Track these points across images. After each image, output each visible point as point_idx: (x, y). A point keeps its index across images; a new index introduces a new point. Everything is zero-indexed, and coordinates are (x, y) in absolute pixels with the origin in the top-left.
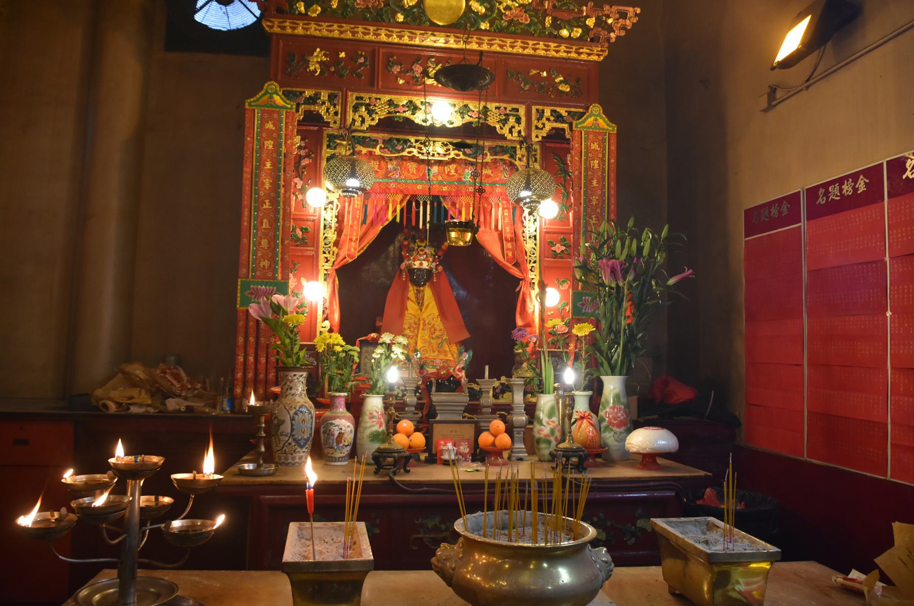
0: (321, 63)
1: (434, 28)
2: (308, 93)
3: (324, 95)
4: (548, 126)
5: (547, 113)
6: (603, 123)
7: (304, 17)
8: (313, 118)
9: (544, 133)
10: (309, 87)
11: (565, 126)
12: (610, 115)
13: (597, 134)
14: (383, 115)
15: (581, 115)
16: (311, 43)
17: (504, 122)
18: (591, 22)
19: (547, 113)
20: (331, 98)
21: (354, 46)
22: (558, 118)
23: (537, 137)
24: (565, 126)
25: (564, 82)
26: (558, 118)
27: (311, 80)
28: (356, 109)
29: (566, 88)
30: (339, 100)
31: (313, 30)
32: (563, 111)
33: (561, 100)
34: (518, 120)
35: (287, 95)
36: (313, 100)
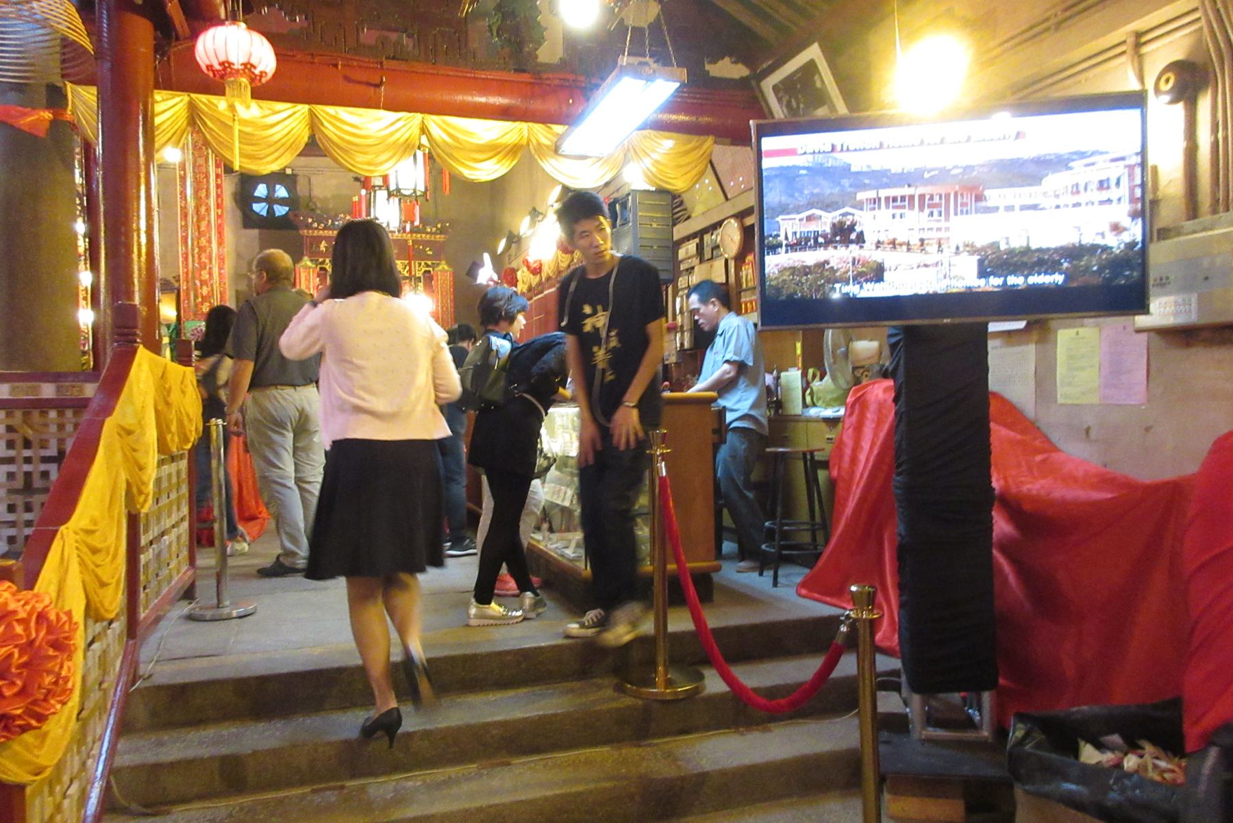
0: (326, 247)
2: (321, 260)
5: (423, 263)
6: (446, 267)
11: (431, 269)
12: (448, 264)
13: (443, 271)
15: (438, 264)
16: (320, 239)
18: (439, 226)
19: (423, 263)
22: (427, 266)
24: (431, 269)
25: (430, 250)
26: (427, 266)
27: (321, 254)
32: (429, 263)
33: (428, 257)
35: (311, 261)
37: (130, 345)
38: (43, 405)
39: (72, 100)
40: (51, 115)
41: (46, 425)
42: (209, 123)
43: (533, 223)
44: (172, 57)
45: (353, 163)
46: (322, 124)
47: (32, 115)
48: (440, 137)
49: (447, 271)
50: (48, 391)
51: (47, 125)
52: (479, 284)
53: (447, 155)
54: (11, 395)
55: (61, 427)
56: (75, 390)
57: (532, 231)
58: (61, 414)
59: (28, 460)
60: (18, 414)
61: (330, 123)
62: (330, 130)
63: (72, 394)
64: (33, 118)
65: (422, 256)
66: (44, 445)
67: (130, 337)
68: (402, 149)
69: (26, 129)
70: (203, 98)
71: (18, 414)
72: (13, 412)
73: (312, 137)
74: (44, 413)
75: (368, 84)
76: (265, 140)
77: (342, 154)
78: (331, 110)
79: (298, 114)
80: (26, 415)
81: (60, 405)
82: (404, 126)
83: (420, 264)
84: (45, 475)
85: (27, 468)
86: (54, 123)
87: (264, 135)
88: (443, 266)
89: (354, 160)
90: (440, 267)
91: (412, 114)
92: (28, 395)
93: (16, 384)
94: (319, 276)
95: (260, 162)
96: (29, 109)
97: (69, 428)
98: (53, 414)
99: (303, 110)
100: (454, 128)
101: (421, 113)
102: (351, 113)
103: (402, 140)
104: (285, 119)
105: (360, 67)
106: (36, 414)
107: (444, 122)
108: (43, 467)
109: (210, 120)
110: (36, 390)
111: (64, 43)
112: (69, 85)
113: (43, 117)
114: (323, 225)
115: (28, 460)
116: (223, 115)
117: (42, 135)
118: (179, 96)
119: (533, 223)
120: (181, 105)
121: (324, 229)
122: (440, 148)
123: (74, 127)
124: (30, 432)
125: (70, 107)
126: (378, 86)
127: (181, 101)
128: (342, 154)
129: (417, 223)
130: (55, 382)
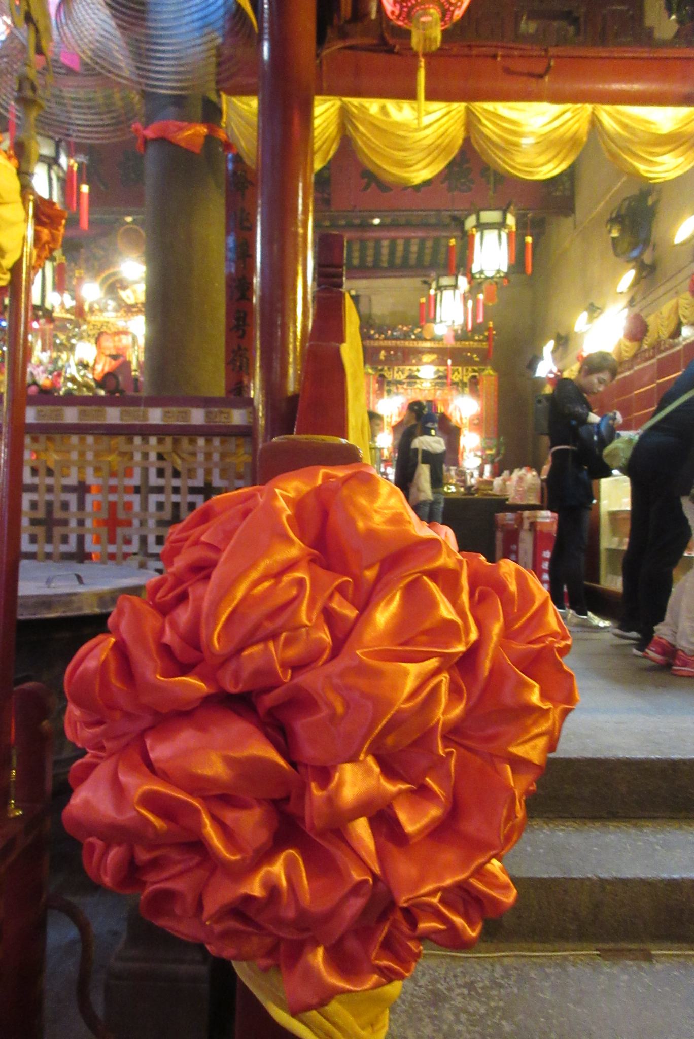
1: (426, 340)
2: (380, 368)
3: (386, 368)
4: (471, 374)
6: (491, 372)
7: (378, 339)
8: (382, 376)
9: (469, 377)
10: (380, 365)
11: (476, 374)
13: (490, 375)
14: (407, 374)
15: (483, 370)
17: (453, 374)
20: (389, 369)
21: (396, 349)
22: (474, 371)
23: (466, 380)
24: (476, 374)
28: (398, 372)
29: (477, 359)
30: (391, 370)
31: (382, 344)
34: (458, 373)
36: (382, 370)
37: (335, 289)
38: (192, 432)
39: (227, 112)
40: (206, 130)
41: (194, 454)
42: (361, 128)
43: (591, 319)
44: (325, 62)
45: (512, 163)
46: (480, 121)
47: (189, 130)
48: (613, 127)
49: (491, 376)
50: (197, 417)
51: (201, 140)
52: (539, 378)
53: (621, 149)
54: (164, 421)
55: (208, 456)
56: (223, 415)
57: (589, 326)
58: (208, 441)
59: (176, 490)
60: (169, 440)
61: (487, 119)
62: (489, 128)
63: (221, 420)
64: (189, 133)
65: (469, 362)
66: (191, 473)
67: (335, 280)
68: (568, 147)
69: (183, 144)
70: (355, 101)
71: (169, 440)
72: (164, 439)
73: (467, 141)
74: (192, 442)
75: (531, 75)
76: (418, 143)
77: (501, 155)
78: (489, 106)
79: (453, 113)
80: (176, 442)
81: (207, 432)
82: (571, 118)
83: (467, 370)
84: (192, 506)
85: (175, 498)
86: (209, 139)
87: (418, 138)
88: (489, 371)
89: (513, 160)
90: (486, 373)
91: (579, 105)
92: (178, 421)
93: (167, 409)
94: (378, 382)
95: (408, 169)
96: (186, 124)
97: (216, 457)
98: (201, 442)
99: (459, 109)
100: (628, 116)
101: (591, 102)
102: (511, 108)
103: (569, 135)
104: (438, 120)
105: (521, 56)
106: (185, 442)
107: (618, 112)
108: (190, 498)
109: (363, 125)
110: (186, 415)
111: (220, 59)
112: (224, 97)
113: (199, 131)
114: (383, 336)
115: (176, 490)
116: (378, 119)
117: (197, 150)
118: (329, 100)
119: (591, 319)
120: (332, 110)
121: (386, 339)
122: (613, 141)
123: (228, 146)
124: (179, 461)
125: (224, 120)
126: (541, 76)
127: (333, 106)
128: (501, 155)
129: (480, 320)
130: (204, 407)
